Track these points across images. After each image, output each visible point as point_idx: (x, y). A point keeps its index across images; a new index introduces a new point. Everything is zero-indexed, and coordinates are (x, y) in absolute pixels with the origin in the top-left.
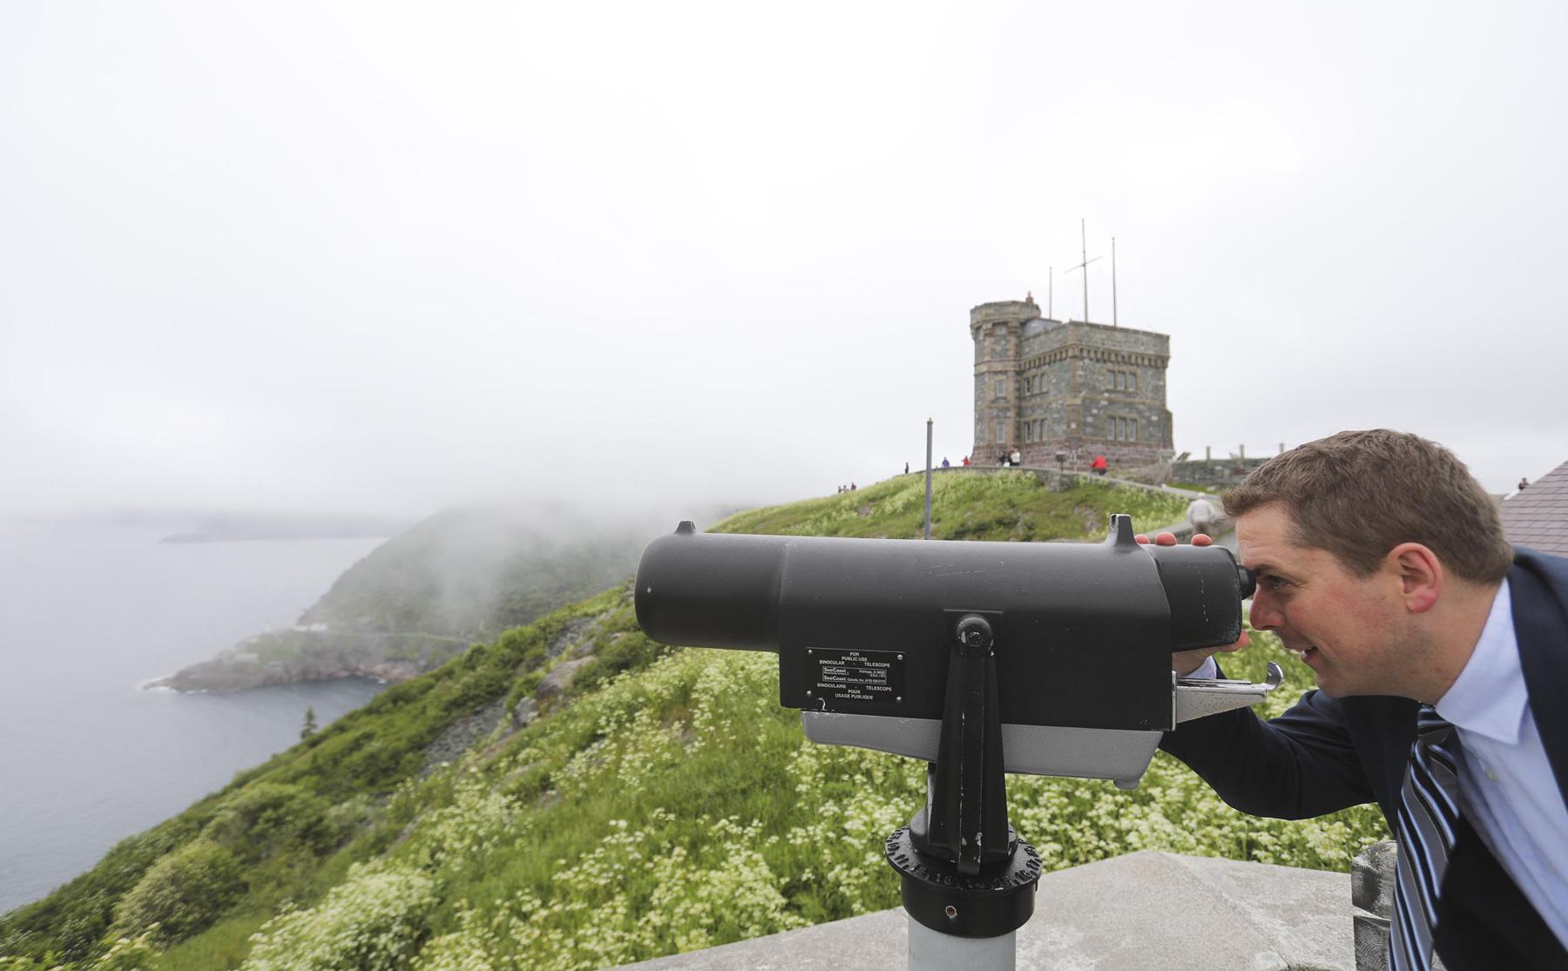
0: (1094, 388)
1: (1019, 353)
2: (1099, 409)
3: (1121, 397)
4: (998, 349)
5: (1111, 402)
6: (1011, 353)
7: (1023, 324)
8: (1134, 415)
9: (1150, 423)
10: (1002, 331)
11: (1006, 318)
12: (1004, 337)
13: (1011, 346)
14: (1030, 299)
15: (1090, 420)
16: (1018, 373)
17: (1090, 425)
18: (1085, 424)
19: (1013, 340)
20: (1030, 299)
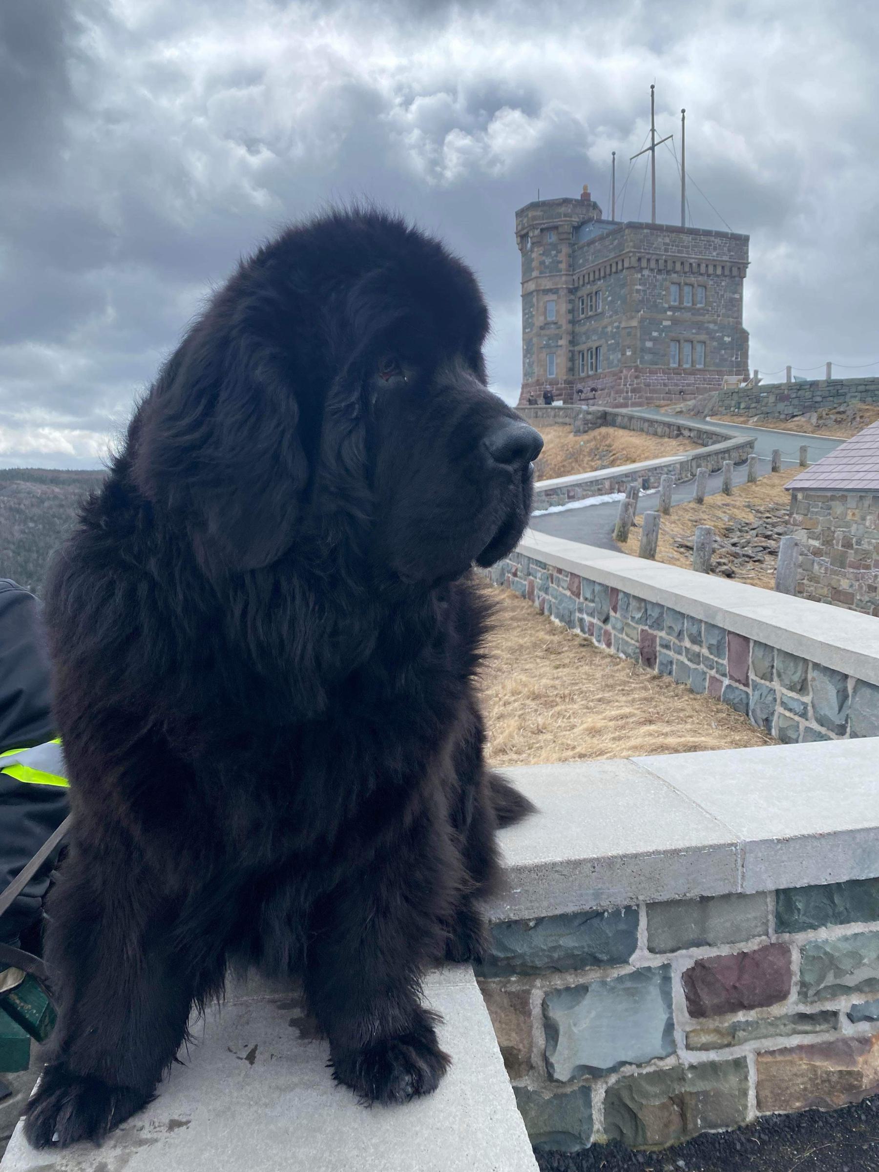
0: (655, 305)
1: (572, 266)
2: (661, 331)
3: (687, 315)
4: (548, 261)
5: (675, 321)
6: (563, 266)
7: (577, 229)
8: (703, 337)
9: (723, 345)
10: (552, 238)
11: (557, 222)
12: (554, 246)
13: (562, 257)
14: (586, 196)
15: (649, 344)
17: (650, 351)
18: (643, 350)
19: (565, 250)
20: (586, 196)
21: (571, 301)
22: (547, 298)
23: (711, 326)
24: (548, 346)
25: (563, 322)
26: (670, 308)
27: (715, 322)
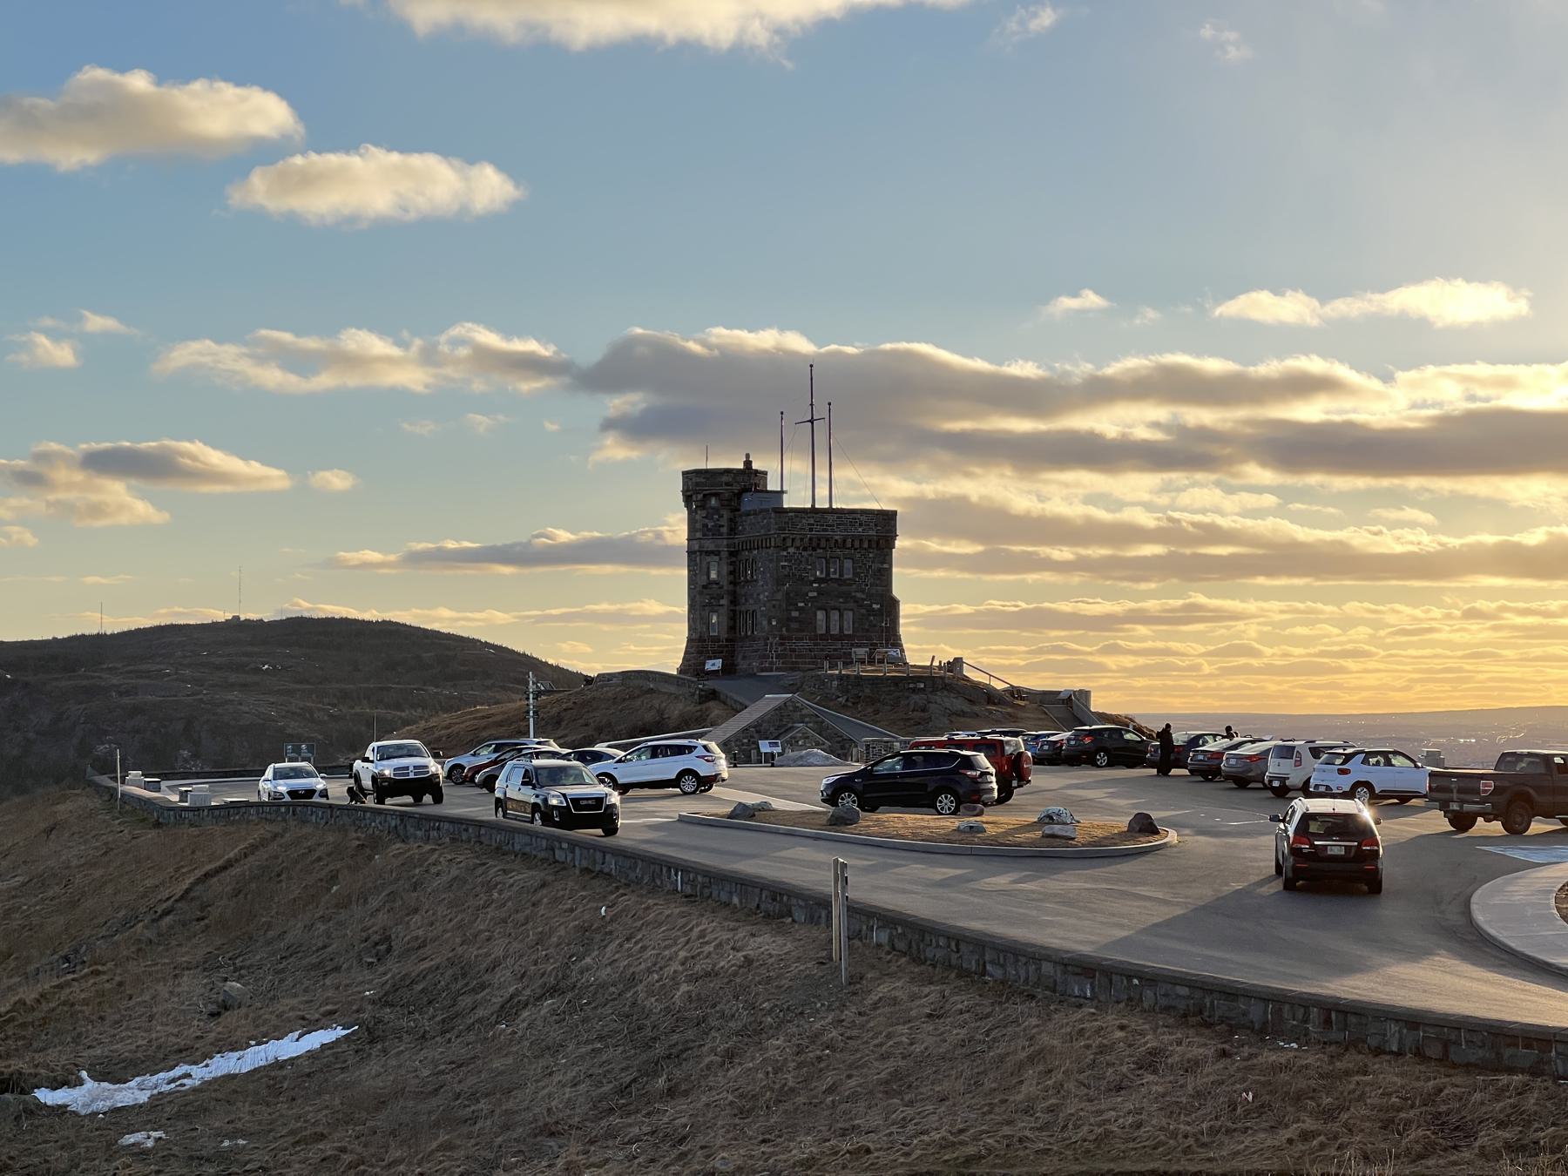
0: (801, 579)
1: (733, 531)
5: (820, 592)
6: (724, 530)
7: (739, 495)
9: (871, 611)
11: (718, 490)
12: (716, 510)
13: (724, 521)
15: (795, 614)
16: (732, 554)
17: (795, 619)
18: (790, 619)
21: (732, 563)
22: (709, 559)
23: (859, 595)
24: (710, 604)
25: (724, 583)
26: (817, 580)
27: (863, 591)
